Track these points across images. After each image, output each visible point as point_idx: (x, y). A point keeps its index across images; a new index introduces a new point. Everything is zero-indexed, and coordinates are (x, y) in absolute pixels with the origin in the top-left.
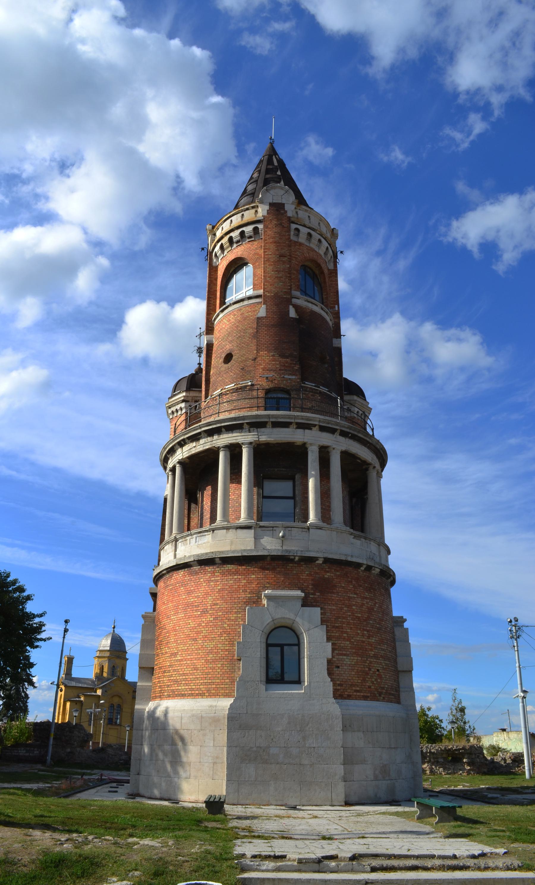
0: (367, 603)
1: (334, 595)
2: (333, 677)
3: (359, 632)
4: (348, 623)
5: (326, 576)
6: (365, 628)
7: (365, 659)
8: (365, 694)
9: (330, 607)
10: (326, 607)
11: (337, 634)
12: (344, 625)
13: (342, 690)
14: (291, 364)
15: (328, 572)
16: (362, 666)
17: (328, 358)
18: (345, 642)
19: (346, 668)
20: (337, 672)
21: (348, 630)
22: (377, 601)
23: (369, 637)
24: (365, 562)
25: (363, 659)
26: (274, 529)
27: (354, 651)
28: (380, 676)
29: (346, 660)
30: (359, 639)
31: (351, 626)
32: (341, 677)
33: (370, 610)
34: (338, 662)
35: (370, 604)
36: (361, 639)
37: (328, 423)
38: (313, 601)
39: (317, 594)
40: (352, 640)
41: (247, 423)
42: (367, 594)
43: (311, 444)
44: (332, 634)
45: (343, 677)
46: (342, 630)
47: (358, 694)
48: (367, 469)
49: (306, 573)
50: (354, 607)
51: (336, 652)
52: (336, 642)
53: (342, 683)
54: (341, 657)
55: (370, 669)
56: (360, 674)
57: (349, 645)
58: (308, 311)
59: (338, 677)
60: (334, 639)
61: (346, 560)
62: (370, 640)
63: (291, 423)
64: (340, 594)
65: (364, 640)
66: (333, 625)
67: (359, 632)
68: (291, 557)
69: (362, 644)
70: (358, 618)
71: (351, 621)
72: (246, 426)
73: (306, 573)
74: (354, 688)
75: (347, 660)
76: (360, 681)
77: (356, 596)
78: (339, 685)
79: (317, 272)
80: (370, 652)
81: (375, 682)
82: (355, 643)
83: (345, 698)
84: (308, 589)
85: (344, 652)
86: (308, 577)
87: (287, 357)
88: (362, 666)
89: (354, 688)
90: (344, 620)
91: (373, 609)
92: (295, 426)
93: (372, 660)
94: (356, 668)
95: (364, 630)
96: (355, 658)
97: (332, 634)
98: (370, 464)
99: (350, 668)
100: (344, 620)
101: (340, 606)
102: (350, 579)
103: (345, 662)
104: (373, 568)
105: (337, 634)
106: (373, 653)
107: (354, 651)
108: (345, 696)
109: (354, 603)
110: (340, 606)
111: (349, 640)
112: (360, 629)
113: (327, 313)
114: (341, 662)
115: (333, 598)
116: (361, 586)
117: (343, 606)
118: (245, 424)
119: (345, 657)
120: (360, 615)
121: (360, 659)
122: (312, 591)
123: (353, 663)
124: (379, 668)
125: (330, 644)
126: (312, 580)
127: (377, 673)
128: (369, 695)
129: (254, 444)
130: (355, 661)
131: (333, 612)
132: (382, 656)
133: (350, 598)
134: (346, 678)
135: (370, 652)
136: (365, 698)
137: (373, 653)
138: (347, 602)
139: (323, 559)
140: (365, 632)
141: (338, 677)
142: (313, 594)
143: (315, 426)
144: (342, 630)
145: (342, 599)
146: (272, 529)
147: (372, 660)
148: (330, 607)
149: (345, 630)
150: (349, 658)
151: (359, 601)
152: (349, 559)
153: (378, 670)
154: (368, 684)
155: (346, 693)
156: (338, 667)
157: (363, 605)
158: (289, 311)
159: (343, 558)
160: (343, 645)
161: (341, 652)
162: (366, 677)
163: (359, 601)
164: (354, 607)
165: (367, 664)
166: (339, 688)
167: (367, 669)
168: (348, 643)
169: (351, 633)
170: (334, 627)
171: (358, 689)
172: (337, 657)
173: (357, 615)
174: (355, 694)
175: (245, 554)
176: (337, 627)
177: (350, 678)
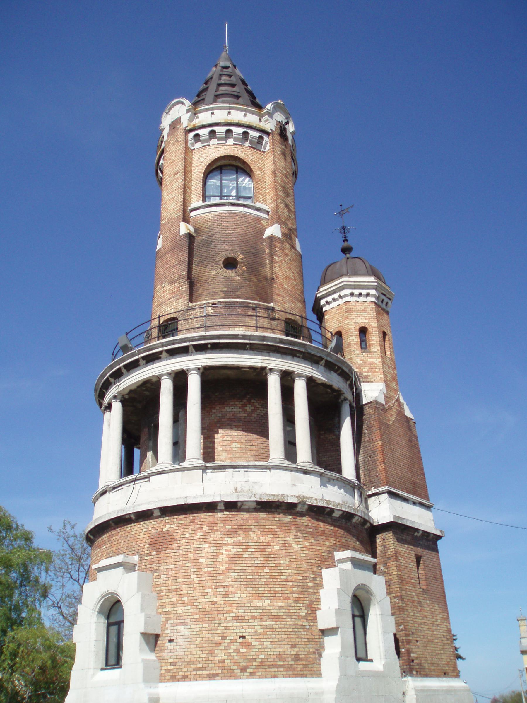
0: (228, 551)
1: (173, 551)
2: (164, 654)
3: (210, 590)
4: (191, 583)
5: (164, 530)
6: (218, 584)
7: (216, 625)
8: (211, 672)
9: (167, 567)
10: (162, 567)
11: (173, 600)
12: (184, 586)
13: (175, 671)
14: (179, 287)
15: (168, 523)
16: (211, 635)
17: (241, 256)
18: (183, 608)
19: (183, 640)
20: (169, 648)
21: (189, 592)
22: (250, 544)
23: (226, 595)
24: (218, 499)
25: (213, 625)
26: (122, 487)
27: (198, 616)
28: (249, 645)
29: (184, 630)
30: (206, 600)
31: (195, 586)
32: (175, 654)
33: (233, 560)
34: (172, 634)
35: (235, 550)
36: (210, 600)
37: (174, 344)
38: (148, 563)
39: (153, 554)
40: (195, 604)
41: (110, 376)
42: (227, 539)
43: (162, 375)
44: (167, 600)
45: (177, 654)
46: (180, 593)
47: (199, 672)
48: (266, 374)
49: (143, 531)
50: (201, 561)
51: (169, 622)
52: (172, 609)
53: (175, 660)
54: (177, 627)
55: (224, 638)
56: (205, 645)
57: (192, 610)
58: (210, 216)
59: (171, 654)
60: (170, 606)
61: (185, 504)
62: (227, 599)
63: (138, 360)
64: (181, 548)
65: (215, 600)
66: (170, 588)
67: (206, 591)
68: (127, 517)
69: (213, 606)
70: (209, 573)
71: (195, 579)
72: (112, 380)
73: (143, 531)
74: (193, 666)
75: (185, 630)
76: (204, 656)
77: (207, 545)
78: (171, 664)
79: (240, 165)
80: (225, 615)
81: (235, 654)
82: (200, 607)
83: (178, 680)
84: (144, 550)
85: (181, 621)
86: (145, 536)
87: (175, 282)
88: (211, 635)
89: (193, 666)
90: (184, 580)
91: (240, 556)
92: (144, 362)
93: (229, 625)
94: (199, 639)
95: (217, 587)
96: (198, 626)
97: (167, 600)
98: (263, 369)
99: (189, 640)
100: (184, 580)
101: (181, 563)
102: (198, 526)
103: (181, 634)
104: (239, 504)
105: (173, 600)
106: (232, 615)
107: (198, 616)
108: (178, 677)
109: (203, 555)
110: (181, 563)
111: (190, 603)
112: (210, 587)
113: (244, 206)
114: (175, 634)
115: (171, 555)
116: (217, 530)
117: (184, 562)
118: (110, 379)
119: (183, 627)
120: (212, 569)
121: (207, 625)
122: (148, 552)
123: (195, 633)
124: (244, 634)
125: (143, 615)
126: (150, 538)
127: (241, 640)
128: (220, 672)
129: (120, 397)
130: (199, 629)
131: (170, 573)
132: (253, 617)
133: (196, 550)
134: (183, 653)
135: (225, 615)
136: (212, 677)
137: (234, 615)
138: (191, 555)
139: (158, 510)
140: (222, 590)
141: (171, 654)
142: (149, 554)
143: (161, 352)
144: (180, 593)
145: (184, 553)
146: (120, 488)
147: (229, 625)
148: (167, 567)
149: (186, 592)
150: (189, 627)
151: (213, 550)
152: (190, 501)
153: (244, 637)
154: (217, 658)
155: (180, 673)
156: (171, 641)
157: (219, 554)
158: (179, 229)
159: (182, 503)
160: (181, 612)
161: (178, 621)
162: (215, 648)
163: (212, 551)
164: (201, 561)
165: (219, 632)
166: (172, 667)
167: (220, 638)
168: (189, 607)
169: (195, 595)
170: (170, 591)
171: (201, 666)
172: (172, 628)
173: (206, 569)
174: (195, 673)
175: (97, 524)
176: (175, 590)
177: (189, 653)
